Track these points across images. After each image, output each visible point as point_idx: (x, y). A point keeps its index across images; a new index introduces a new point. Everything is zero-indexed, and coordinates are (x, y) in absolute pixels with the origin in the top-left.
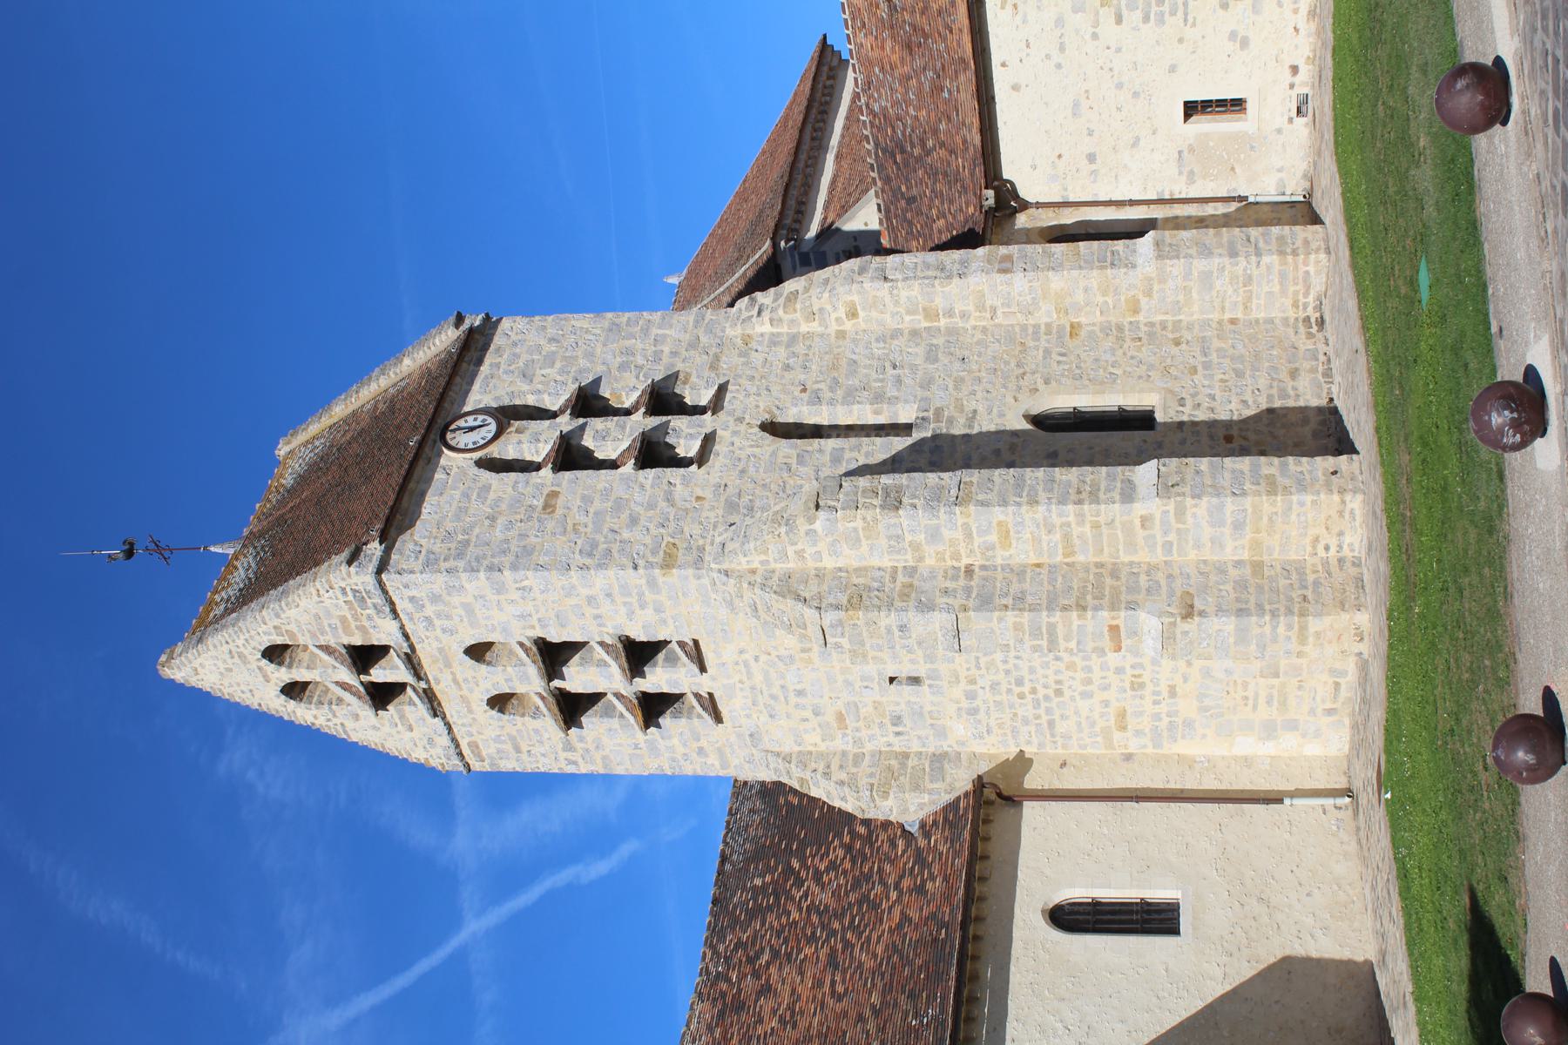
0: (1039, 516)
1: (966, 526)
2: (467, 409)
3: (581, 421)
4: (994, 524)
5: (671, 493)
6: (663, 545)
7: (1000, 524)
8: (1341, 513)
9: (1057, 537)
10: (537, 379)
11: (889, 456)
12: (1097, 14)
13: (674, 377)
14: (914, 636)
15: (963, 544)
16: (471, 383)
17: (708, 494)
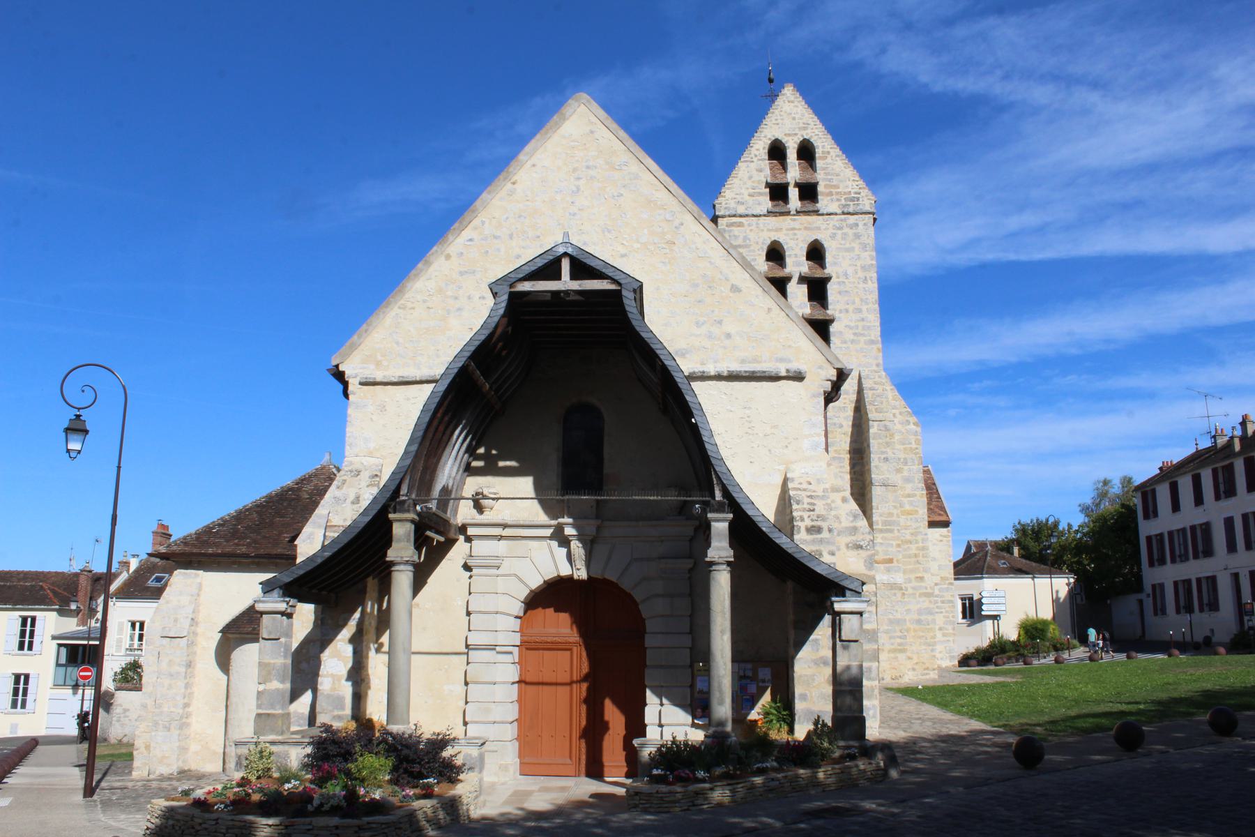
0: (922, 530)
1: (914, 495)
4: (916, 509)
7: (917, 511)
8: (927, 669)
9: (908, 537)
12: (938, 575)
14: (880, 464)
15: (902, 493)
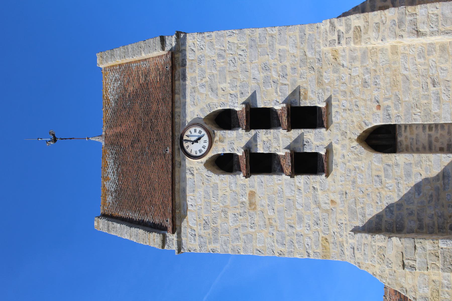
2: (189, 119)
3: (253, 132)
5: (315, 196)
6: (320, 239)
10: (220, 92)
11: (440, 171)
13: (296, 92)
16: (184, 96)
17: (337, 198)
